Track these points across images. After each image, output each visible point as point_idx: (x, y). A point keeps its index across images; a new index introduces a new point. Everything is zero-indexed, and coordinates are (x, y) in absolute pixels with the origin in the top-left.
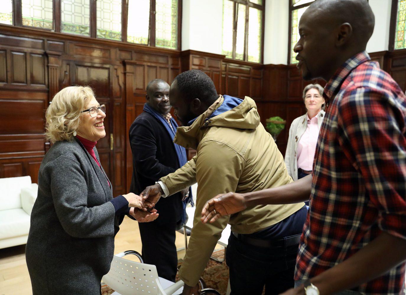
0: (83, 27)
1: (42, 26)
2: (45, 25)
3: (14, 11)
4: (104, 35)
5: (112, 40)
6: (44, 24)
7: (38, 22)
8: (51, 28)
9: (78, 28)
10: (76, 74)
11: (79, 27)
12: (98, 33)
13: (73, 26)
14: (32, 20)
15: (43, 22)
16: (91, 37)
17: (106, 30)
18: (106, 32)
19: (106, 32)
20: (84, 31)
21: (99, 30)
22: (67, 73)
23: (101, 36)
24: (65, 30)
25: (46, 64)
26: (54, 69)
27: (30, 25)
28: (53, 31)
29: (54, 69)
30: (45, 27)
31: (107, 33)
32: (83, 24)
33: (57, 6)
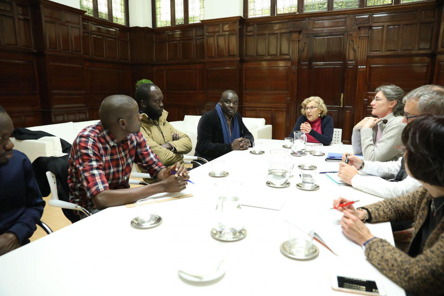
0: (321, 4)
1: (290, 12)
4: (341, 6)
5: (349, 8)
7: (287, 9)
8: (296, 11)
9: (317, 6)
11: (318, 5)
12: (335, 6)
13: (313, 5)
15: (291, 8)
16: (328, 11)
17: (342, 1)
18: (343, 3)
20: (323, 7)
23: (338, 8)
24: (306, 10)
27: (282, 13)
28: (298, 13)
29: (293, 42)
30: (292, 11)
31: (344, 4)
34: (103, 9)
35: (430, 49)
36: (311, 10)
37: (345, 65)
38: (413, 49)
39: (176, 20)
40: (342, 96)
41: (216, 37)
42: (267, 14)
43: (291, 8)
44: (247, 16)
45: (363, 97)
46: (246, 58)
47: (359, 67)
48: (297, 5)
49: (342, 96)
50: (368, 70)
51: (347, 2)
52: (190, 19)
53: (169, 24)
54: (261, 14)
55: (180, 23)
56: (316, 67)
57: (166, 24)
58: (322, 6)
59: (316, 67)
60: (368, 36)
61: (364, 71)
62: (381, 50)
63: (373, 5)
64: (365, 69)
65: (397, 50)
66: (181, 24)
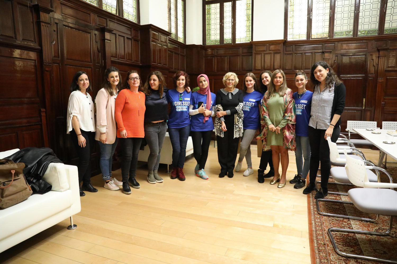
0: (348, 32)
1: (322, 37)
2: (324, 36)
3: (307, 32)
6: (323, 35)
8: (328, 37)
9: (344, 33)
10: (342, 61)
11: (346, 32)
12: (359, 33)
13: (342, 33)
14: (317, 34)
15: (323, 34)
16: (353, 37)
17: (365, 30)
18: (365, 31)
19: (365, 31)
20: (349, 34)
21: (360, 31)
22: (335, 62)
24: (335, 36)
25: (323, 58)
26: (325, 60)
27: (316, 37)
30: (324, 37)
31: (366, 32)
32: (348, 30)
33: (332, 23)
34: (173, 31)
36: (340, 36)
39: (224, 40)
40: (364, 100)
41: (263, 55)
42: (304, 38)
43: (323, 34)
44: (287, 39)
45: (382, 101)
48: (328, 32)
49: (364, 100)
51: (369, 31)
52: (237, 40)
53: (218, 43)
54: (299, 38)
55: (228, 43)
57: (215, 43)
58: (348, 33)
61: (382, 82)
63: (389, 33)
66: (229, 44)
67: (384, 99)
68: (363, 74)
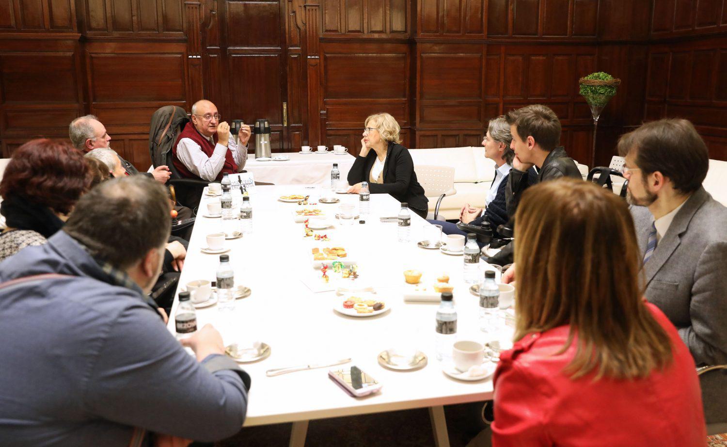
35: (406, 32)
37: (285, 54)
38: (384, 31)
46: (89, 34)
47: (308, 57)
50: (322, 61)
56: (234, 55)
59: (234, 55)
60: (318, 6)
61: (317, 65)
62: (339, 28)
64: (318, 61)
65: (362, 31)
67: (325, 103)
68: (278, 47)
